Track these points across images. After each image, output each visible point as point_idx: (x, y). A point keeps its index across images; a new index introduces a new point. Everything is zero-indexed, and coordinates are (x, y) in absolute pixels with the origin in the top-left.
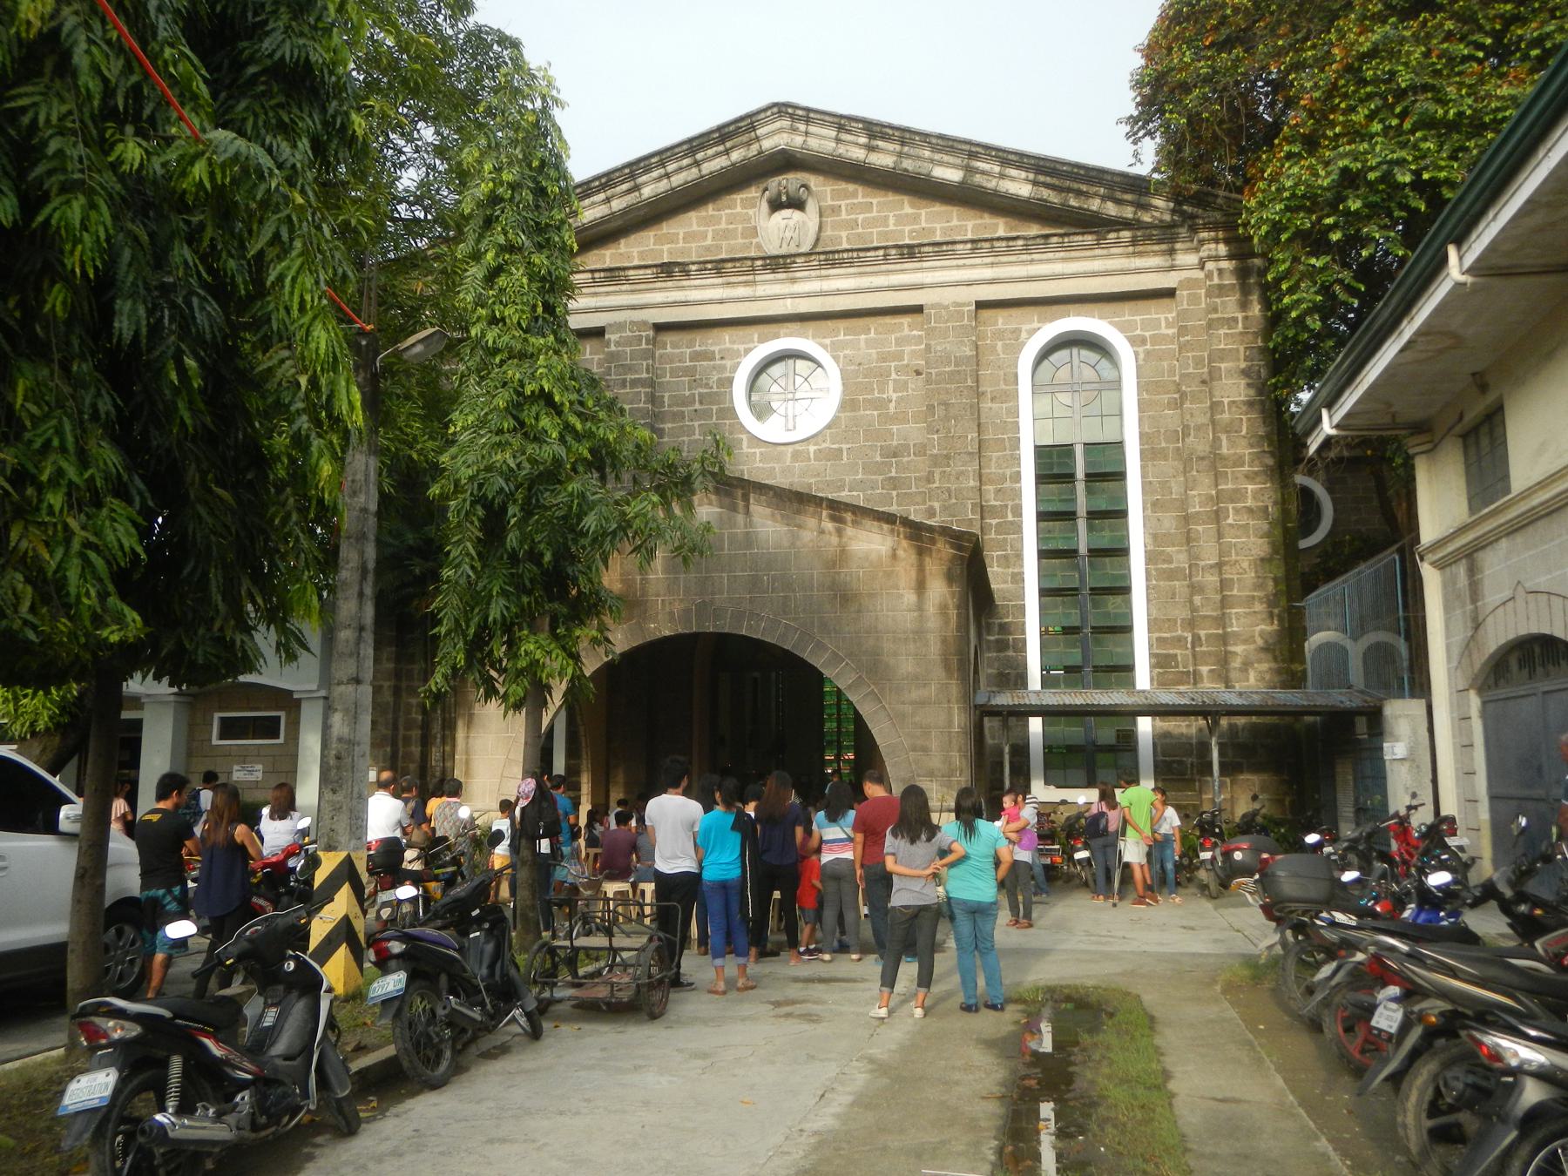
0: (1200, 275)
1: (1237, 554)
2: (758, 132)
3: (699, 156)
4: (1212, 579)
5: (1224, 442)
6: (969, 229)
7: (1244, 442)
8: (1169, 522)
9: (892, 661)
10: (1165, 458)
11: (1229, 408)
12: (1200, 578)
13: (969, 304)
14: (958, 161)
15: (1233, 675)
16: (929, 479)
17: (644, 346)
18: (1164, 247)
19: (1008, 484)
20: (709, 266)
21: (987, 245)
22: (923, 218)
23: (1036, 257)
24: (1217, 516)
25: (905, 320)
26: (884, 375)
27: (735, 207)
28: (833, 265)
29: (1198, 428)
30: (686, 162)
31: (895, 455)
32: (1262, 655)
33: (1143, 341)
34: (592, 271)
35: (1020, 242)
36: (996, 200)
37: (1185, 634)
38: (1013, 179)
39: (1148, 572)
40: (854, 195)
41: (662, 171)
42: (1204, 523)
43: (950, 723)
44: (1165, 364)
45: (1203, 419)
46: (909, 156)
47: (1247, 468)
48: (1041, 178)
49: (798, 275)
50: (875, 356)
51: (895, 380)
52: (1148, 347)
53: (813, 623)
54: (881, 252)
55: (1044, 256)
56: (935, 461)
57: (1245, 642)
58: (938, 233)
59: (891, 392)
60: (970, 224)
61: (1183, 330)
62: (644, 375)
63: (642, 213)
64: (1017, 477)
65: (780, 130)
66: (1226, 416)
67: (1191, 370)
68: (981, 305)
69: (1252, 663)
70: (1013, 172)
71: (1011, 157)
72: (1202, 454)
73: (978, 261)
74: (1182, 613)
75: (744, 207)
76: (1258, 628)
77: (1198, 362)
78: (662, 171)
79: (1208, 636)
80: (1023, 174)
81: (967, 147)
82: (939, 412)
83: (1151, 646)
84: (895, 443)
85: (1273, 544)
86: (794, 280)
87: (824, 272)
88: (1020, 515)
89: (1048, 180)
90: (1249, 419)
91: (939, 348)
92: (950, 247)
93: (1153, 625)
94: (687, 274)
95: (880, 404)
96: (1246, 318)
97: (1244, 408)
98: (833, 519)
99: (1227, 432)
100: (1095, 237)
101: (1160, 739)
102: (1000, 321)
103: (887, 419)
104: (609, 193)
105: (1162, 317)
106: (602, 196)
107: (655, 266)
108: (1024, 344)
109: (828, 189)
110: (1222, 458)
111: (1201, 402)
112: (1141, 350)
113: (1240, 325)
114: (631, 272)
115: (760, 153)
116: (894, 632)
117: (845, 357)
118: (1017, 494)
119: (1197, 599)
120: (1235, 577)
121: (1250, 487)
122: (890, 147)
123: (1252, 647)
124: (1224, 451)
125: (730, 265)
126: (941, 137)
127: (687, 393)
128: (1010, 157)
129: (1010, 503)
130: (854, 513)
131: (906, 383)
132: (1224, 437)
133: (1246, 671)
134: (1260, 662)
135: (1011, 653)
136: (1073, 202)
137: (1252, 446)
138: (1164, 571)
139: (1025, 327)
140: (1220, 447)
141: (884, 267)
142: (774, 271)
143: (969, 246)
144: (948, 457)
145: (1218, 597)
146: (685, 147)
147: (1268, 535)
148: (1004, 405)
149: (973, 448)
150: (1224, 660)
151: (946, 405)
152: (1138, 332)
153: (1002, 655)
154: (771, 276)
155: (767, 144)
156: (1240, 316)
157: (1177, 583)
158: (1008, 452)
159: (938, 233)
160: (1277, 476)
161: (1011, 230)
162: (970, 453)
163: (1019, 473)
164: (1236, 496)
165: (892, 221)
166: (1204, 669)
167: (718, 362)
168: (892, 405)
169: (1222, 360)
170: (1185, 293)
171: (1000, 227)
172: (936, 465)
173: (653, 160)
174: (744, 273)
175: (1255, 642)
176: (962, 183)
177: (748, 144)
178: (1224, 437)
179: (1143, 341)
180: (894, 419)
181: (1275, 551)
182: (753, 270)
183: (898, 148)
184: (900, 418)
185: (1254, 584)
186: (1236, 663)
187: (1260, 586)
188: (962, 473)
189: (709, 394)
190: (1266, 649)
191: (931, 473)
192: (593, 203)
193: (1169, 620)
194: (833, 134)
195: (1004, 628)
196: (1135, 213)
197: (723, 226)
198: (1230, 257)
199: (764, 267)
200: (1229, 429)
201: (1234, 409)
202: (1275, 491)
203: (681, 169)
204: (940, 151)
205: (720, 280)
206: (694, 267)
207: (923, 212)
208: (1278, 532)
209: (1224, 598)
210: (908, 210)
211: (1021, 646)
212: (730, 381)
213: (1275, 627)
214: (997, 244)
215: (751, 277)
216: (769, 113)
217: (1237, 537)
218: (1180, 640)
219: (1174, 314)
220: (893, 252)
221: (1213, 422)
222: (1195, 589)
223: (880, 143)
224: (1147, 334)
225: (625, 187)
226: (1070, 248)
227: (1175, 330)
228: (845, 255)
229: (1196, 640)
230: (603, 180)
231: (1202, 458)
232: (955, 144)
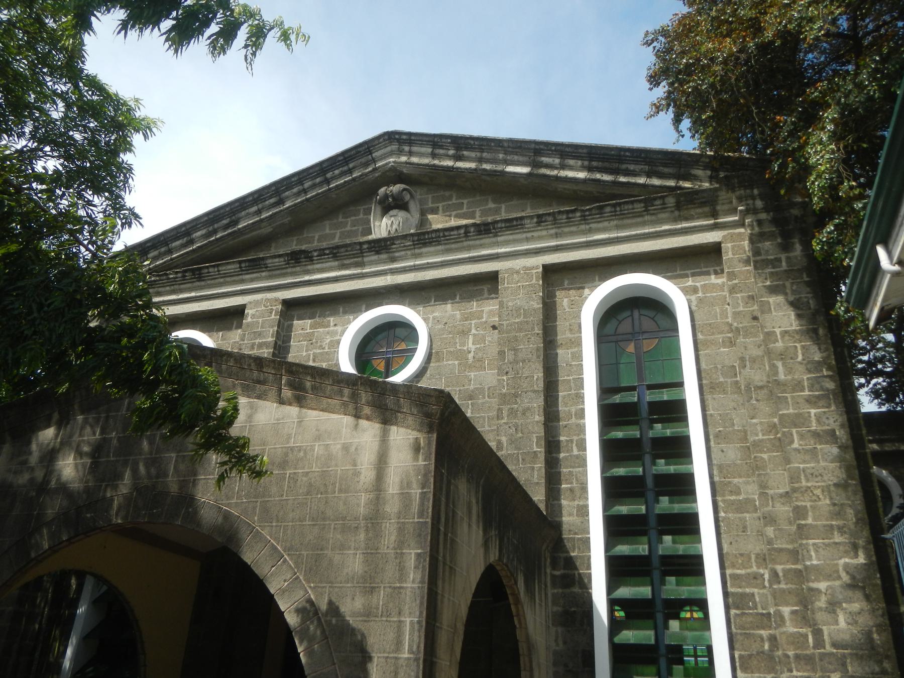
1: (808, 480)
2: (374, 155)
3: (329, 175)
4: (783, 510)
5: (781, 369)
7: (801, 368)
8: (731, 453)
9: (337, 558)
10: (724, 392)
11: (783, 336)
12: (770, 508)
13: (537, 267)
14: (525, 159)
15: (820, 616)
16: (499, 417)
17: (273, 317)
18: (707, 209)
19: (573, 420)
20: (327, 252)
21: (550, 218)
22: (503, 210)
23: (593, 226)
24: (781, 444)
26: (465, 333)
27: (359, 215)
28: (425, 244)
29: (753, 360)
30: (318, 180)
31: (471, 398)
32: (850, 593)
33: (695, 290)
34: (240, 262)
35: (578, 214)
36: (560, 186)
37: (761, 571)
38: (571, 168)
40: (450, 198)
41: (300, 187)
42: (769, 451)
43: (399, 643)
45: (757, 352)
46: (488, 161)
47: (807, 393)
48: (594, 164)
49: (397, 254)
50: (458, 317)
51: (474, 335)
52: (700, 294)
53: (254, 508)
55: (600, 225)
56: (503, 399)
57: (829, 577)
59: (470, 345)
62: (270, 339)
63: (286, 220)
64: (581, 414)
65: (391, 154)
66: (780, 344)
67: (741, 309)
68: (549, 271)
69: (840, 603)
70: (571, 162)
72: (760, 384)
75: (365, 214)
76: (842, 561)
78: (300, 187)
79: (786, 572)
80: (580, 163)
81: (533, 146)
82: (510, 356)
84: (472, 387)
85: (848, 469)
86: (393, 260)
87: (417, 251)
88: (585, 450)
90: (803, 347)
91: (510, 304)
94: (310, 259)
95: (461, 356)
96: (788, 258)
97: (797, 337)
98: (292, 386)
99: (782, 359)
100: (643, 205)
103: (465, 366)
104: (260, 206)
106: (255, 208)
107: (287, 255)
108: (586, 298)
109: (430, 196)
110: (778, 383)
111: (755, 336)
112: (693, 298)
113: (784, 264)
114: (270, 261)
115: (375, 170)
116: (344, 519)
117: (434, 318)
119: (770, 531)
120: (808, 504)
121: (813, 411)
122: (473, 154)
123: (837, 583)
124: (782, 377)
125: (343, 250)
126: (511, 141)
127: (304, 354)
128: (567, 149)
129: (575, 438)
130: (313, 376)
131: (484, 336)
132: (779, 364)
133: (834, 612)
134: (849, 601)
135: (576, 590)
136: (622, 179)
137: (810, 371)
138: (732, 503)
140: (776, 373)
141: (465, 244)
142: (378, 253)
144: (516, 396)
146: (317, 169)
147: (840, 459)
148: (569, 351)
150: (805, 600)
151: (515, 350)
153: (567, 591)
154: (375, 257)
155: (379, 164)
156: (783, 257)
157: (747, 515)
158: (573, 392)
160: (840, 399)
162: (534, 391)
163: (583, 410)
164: (798, 420)
165: (478, 214)
167: (332, 328)
168: (471, 356)
170: (729, 245)
172: (504, 403)
173: (293, 179)
174: (355, 257)
175: (839, 578)
176: (529, 175)
177: (366, 165)
178: (779, 364)
180: (471, 367)
181: (850, 476)
182: (361, 253)
183: (479, 154)
184: (478, 363)
185: (830, 512)
186: (822, 603)
187: (838, 514)
188: (528, 409)
189: (322, 354)
190: (852, 586)
191: (500, 410)
192: (248, 214)
193: (742, 555)
194: (430, 150)
195: (570, 563)
197: (348, 228)
198: (766, 209)
199: (370, 250)
200: (782, 356)
201: (787, 338)
202: (841, 415)
203: (314, 186)
204: (512, 153)
205: (336, 263)
206: (315, 254)
207: (503, 206)
208: (850, 456)
209: (800, 527)
210: (491, 205)
211: (584, 584)
212: (338, 342)
213: (861, 559)
215: (360, 259)
216: (381, 140)
217: (804, 462)
218: (756, 577)
221: (769, 352)
223: (465, 153)
224: (698, 284)
225: (272, 201)
226: (622, 216)
228: (434, 235)
229: (774, 574)
230: (256, 196)
231: (761, 388)
232: (523, 145)
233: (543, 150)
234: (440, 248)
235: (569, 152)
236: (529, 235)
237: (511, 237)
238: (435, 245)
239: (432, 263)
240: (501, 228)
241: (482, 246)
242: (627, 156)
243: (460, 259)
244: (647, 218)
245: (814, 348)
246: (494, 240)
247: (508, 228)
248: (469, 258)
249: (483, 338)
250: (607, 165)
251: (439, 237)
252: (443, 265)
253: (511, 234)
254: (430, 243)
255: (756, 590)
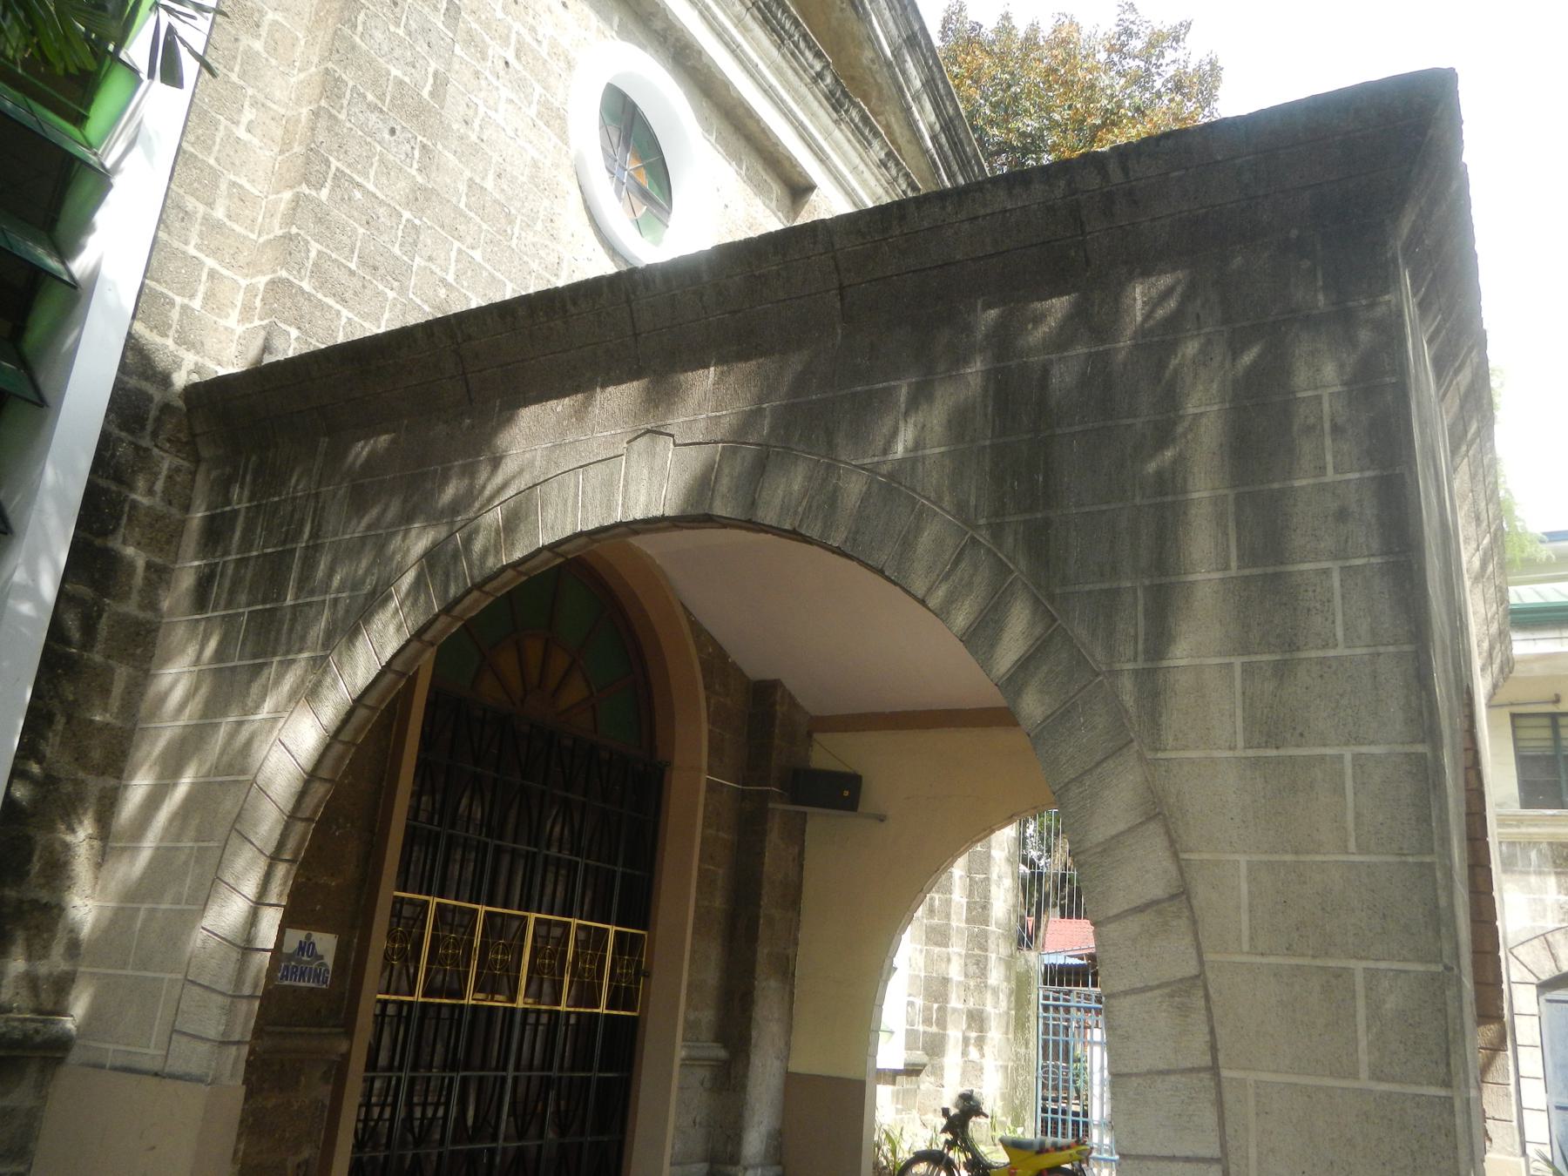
38: (922, 110)
48: (943, 140)
70: (928, 106)
80: (933, 118)
87: (748, 19)
89: (946, 147)
141: (804, 90)
233: (920, 48)
234: (774, 52)
235: (938, 90)
236: (862, 167)
238: (773, 42)
239: (759, 72)
240: (852, 120)
241: (813, 115)
242: (973, 171)
243: (791, 111)
246: (832, 126)
248: (801, 124)
251: (791, 37)
252: (768, 91)
253: (849, 141)
254: (774, 30)
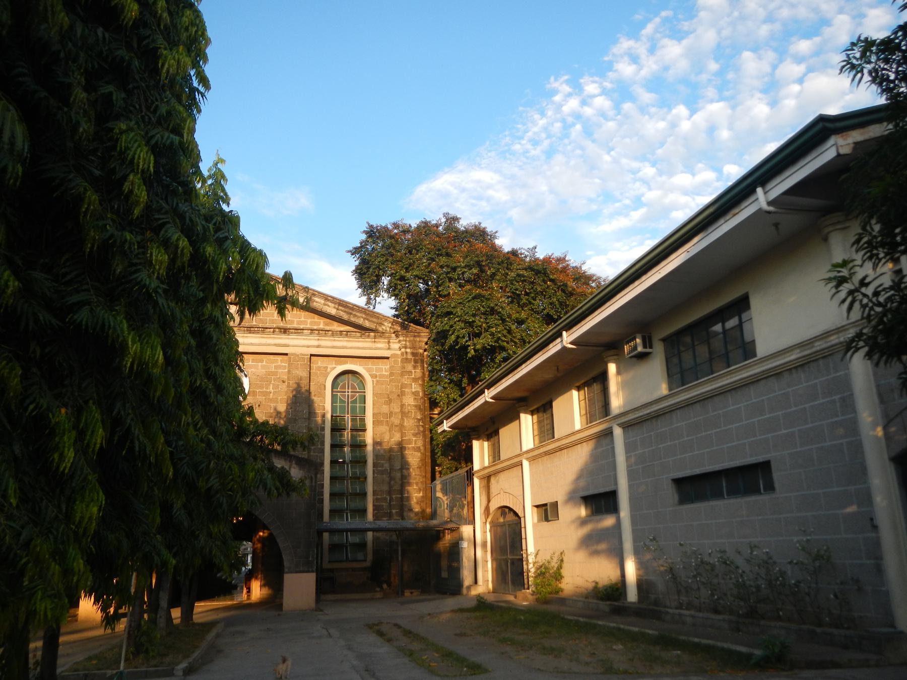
0: (399, 353)
4: (398, 475)
6: (309, 322)
10: (382, 425)
13: (307, 355)
18: (386, 340)
21: (317, 332)
25: (279, 358)
28: (250, 333)
38: (329, 306)
39: (374, 471)
44: (384, 386)
54: (272, 330)
55: (339, 339)
58: (295, 323)
59: (271, 389)
60: (309, 321)
61: (392, 374)
70: (330, 304)
71: (330, 298)
73: (313, 338)
74: (385, 488)
77: (397, 387)
80: (333, 305)
83: (373, 502)
87: (245, 335)
88: (324, 445)
89: (343, 309)
92: (301, 331)
93: (375, 493)
101: (375, 539)
102: (319, 363)
105: (384, 367)
112: (375, 380)
118: (323, 436)
131: (278, 385)
139: (330, 366)
143: (309, 331)
144: (295, 420)
145: (400, 482)
149: (306, 416)
152: (374, 373)
159: (295, 323)
161: (326, 324)
166: (394, 511)
168: (272, 394)
169: (405, 388)
171: (321, 323)
179: (376, 377)
196: (376, 326)
214: (320, 332)
218: (385, 499)
219: (388, 367)
220: (277, 330)
222: (391, 478)
224: (378, 374)
227: (388, 373)
228: (256, 329)
231: (396, 426)
234: (258, 335)
236: (305, 337)
237: (295, 337)
244: (361, 339)
245: (418, 413)
247: (295, 333)
249: (277, 387)
250: (347, 310)
255: (384, 504)
